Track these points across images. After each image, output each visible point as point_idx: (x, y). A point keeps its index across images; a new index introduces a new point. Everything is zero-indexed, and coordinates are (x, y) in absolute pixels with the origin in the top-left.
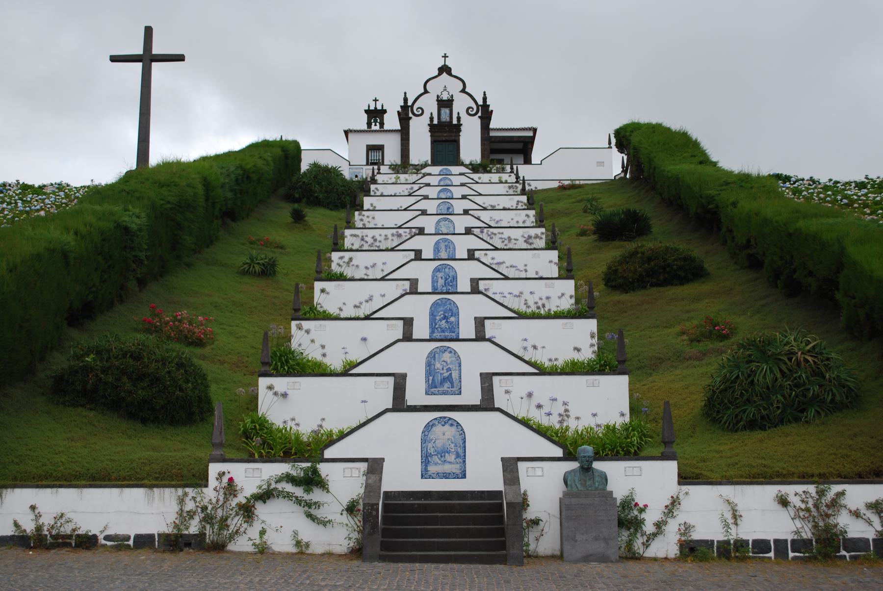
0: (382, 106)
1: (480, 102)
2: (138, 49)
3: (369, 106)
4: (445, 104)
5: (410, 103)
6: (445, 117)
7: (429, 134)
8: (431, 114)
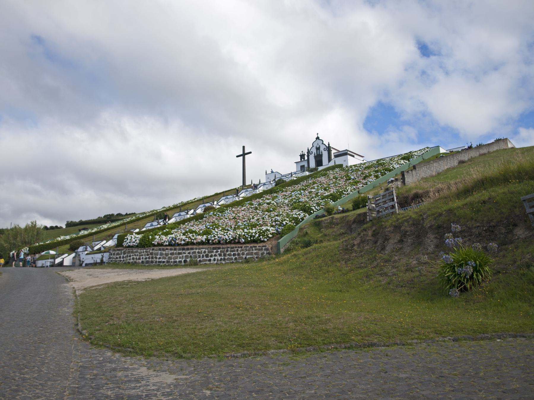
1: (327, 146)
4: (318, 149)
6: (318, 153)
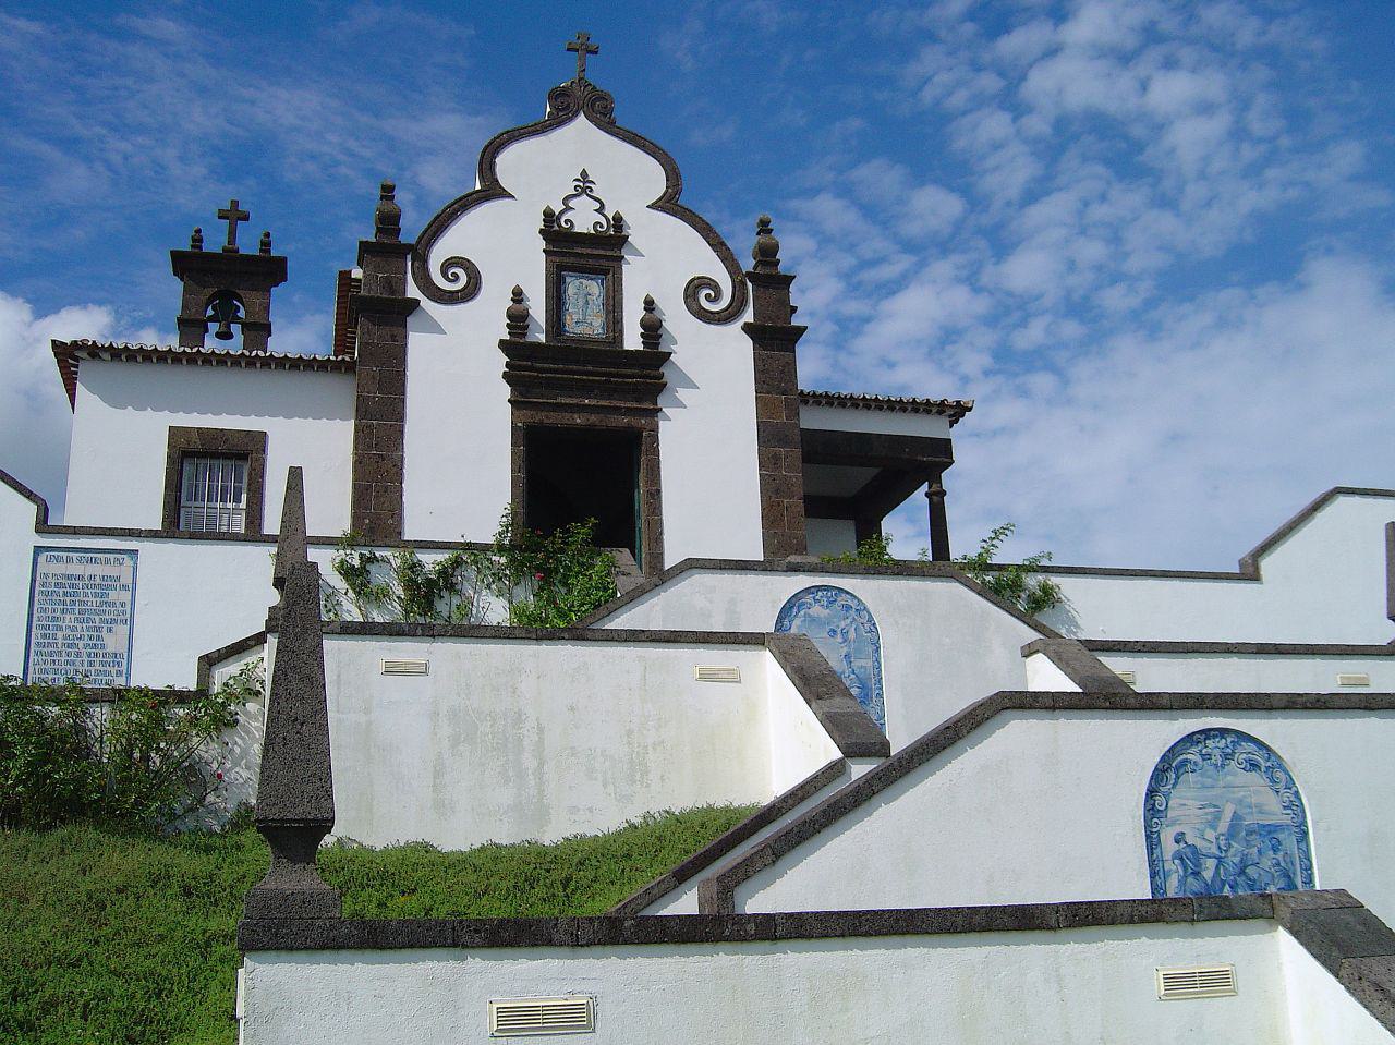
0: (266, 245)
3: (197, 240)
6: (585, 320)
7: (506, 391)
8: (518, 296)
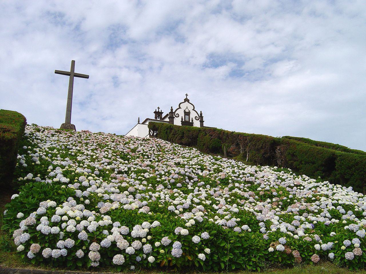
0: (161, 111)
2: (69, 70)
3: (156, 110)
4: (187, 114)
5: (174, 111)
6: (187, 120)
